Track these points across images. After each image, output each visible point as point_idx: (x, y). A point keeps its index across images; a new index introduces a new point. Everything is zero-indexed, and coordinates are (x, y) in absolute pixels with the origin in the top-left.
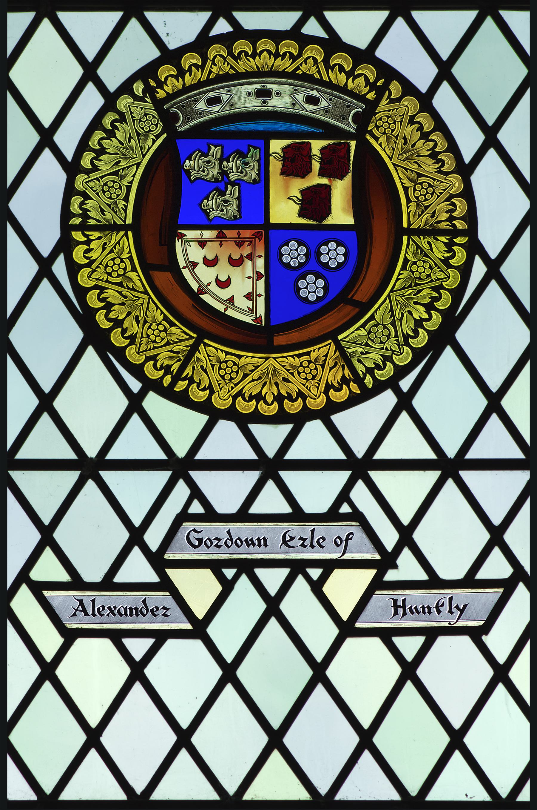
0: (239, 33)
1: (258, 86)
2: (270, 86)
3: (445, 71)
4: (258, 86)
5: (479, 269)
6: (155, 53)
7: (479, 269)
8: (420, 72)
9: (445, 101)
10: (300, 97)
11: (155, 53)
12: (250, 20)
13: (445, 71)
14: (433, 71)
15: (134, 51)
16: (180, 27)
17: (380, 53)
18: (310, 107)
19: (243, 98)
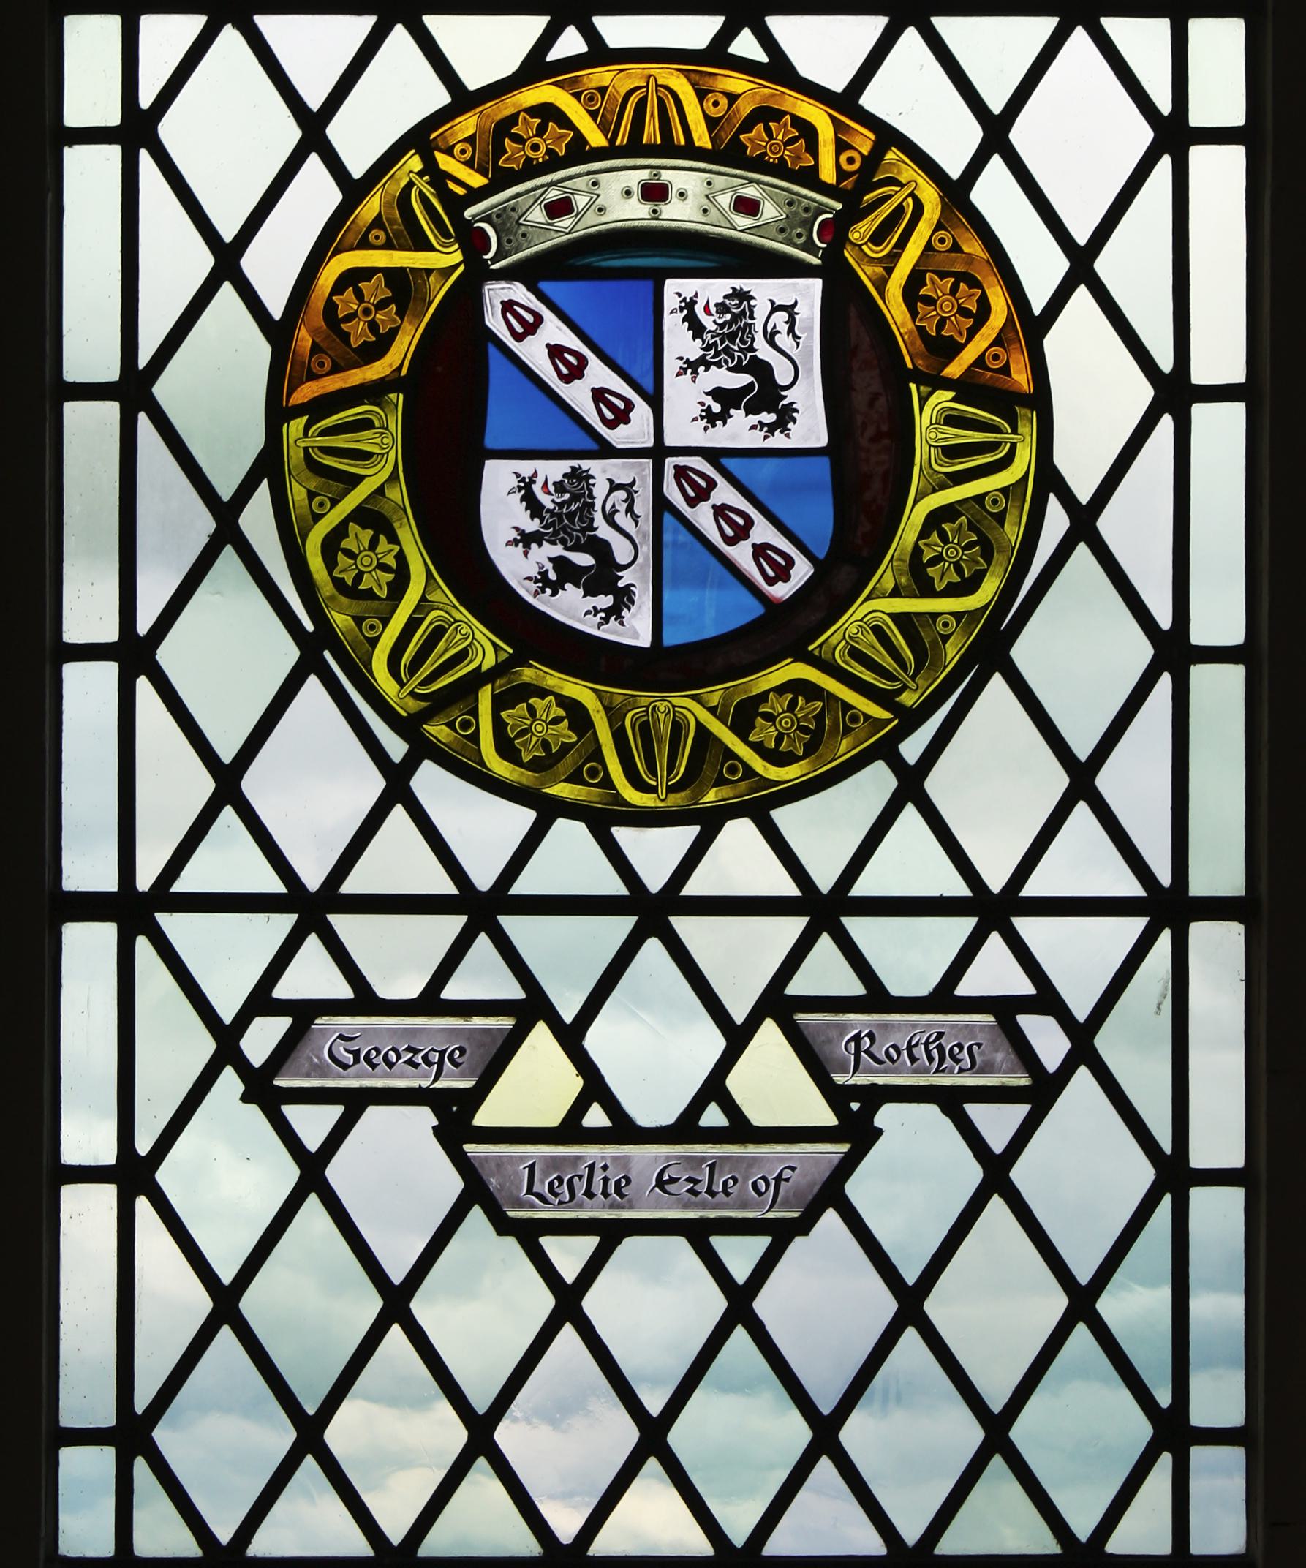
0: (599, 53)
1: (644, 175)
2: (666, 176)
3: (996, 133)
4: (644, 175)
5: (1056, 521)
6: (442, 97)
7: (1056, 521)
8: (950, 137)
9: (996, 194)
10: (725, 200)
11: (442, 97)
12: (619, 30)
13: (996, 133)
14: (974, 134)
15: (399, 92)
16: (488, 46)
17: (870, 100)
18: (743, 221)
19: (614, 199)
